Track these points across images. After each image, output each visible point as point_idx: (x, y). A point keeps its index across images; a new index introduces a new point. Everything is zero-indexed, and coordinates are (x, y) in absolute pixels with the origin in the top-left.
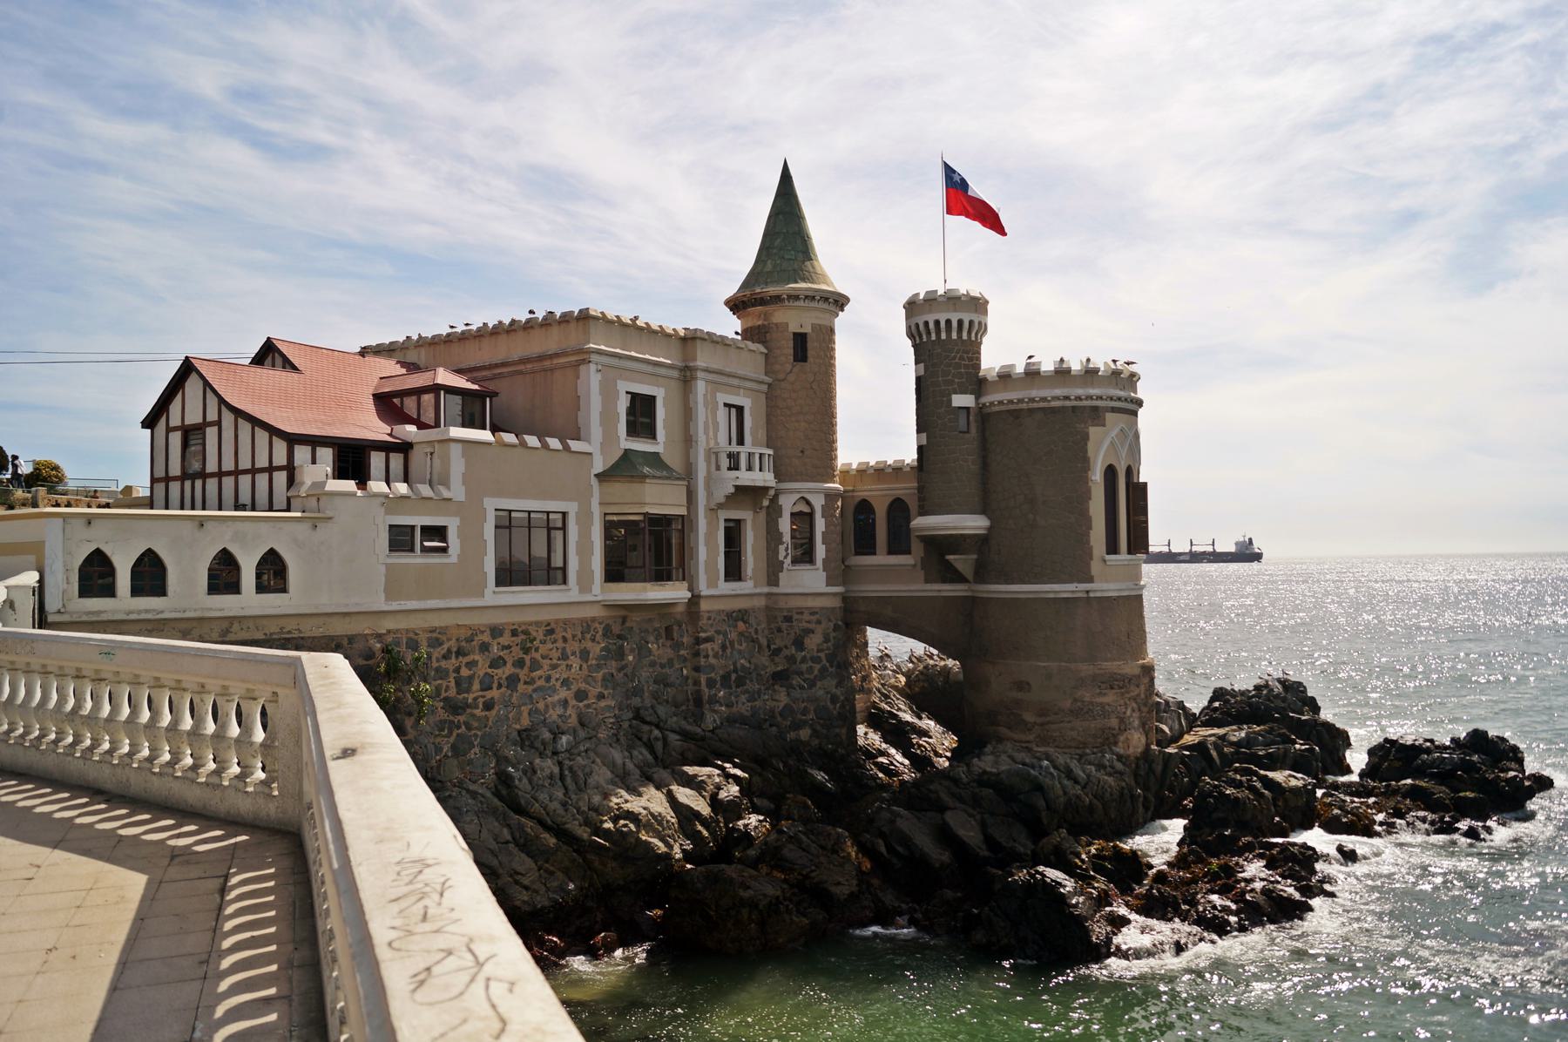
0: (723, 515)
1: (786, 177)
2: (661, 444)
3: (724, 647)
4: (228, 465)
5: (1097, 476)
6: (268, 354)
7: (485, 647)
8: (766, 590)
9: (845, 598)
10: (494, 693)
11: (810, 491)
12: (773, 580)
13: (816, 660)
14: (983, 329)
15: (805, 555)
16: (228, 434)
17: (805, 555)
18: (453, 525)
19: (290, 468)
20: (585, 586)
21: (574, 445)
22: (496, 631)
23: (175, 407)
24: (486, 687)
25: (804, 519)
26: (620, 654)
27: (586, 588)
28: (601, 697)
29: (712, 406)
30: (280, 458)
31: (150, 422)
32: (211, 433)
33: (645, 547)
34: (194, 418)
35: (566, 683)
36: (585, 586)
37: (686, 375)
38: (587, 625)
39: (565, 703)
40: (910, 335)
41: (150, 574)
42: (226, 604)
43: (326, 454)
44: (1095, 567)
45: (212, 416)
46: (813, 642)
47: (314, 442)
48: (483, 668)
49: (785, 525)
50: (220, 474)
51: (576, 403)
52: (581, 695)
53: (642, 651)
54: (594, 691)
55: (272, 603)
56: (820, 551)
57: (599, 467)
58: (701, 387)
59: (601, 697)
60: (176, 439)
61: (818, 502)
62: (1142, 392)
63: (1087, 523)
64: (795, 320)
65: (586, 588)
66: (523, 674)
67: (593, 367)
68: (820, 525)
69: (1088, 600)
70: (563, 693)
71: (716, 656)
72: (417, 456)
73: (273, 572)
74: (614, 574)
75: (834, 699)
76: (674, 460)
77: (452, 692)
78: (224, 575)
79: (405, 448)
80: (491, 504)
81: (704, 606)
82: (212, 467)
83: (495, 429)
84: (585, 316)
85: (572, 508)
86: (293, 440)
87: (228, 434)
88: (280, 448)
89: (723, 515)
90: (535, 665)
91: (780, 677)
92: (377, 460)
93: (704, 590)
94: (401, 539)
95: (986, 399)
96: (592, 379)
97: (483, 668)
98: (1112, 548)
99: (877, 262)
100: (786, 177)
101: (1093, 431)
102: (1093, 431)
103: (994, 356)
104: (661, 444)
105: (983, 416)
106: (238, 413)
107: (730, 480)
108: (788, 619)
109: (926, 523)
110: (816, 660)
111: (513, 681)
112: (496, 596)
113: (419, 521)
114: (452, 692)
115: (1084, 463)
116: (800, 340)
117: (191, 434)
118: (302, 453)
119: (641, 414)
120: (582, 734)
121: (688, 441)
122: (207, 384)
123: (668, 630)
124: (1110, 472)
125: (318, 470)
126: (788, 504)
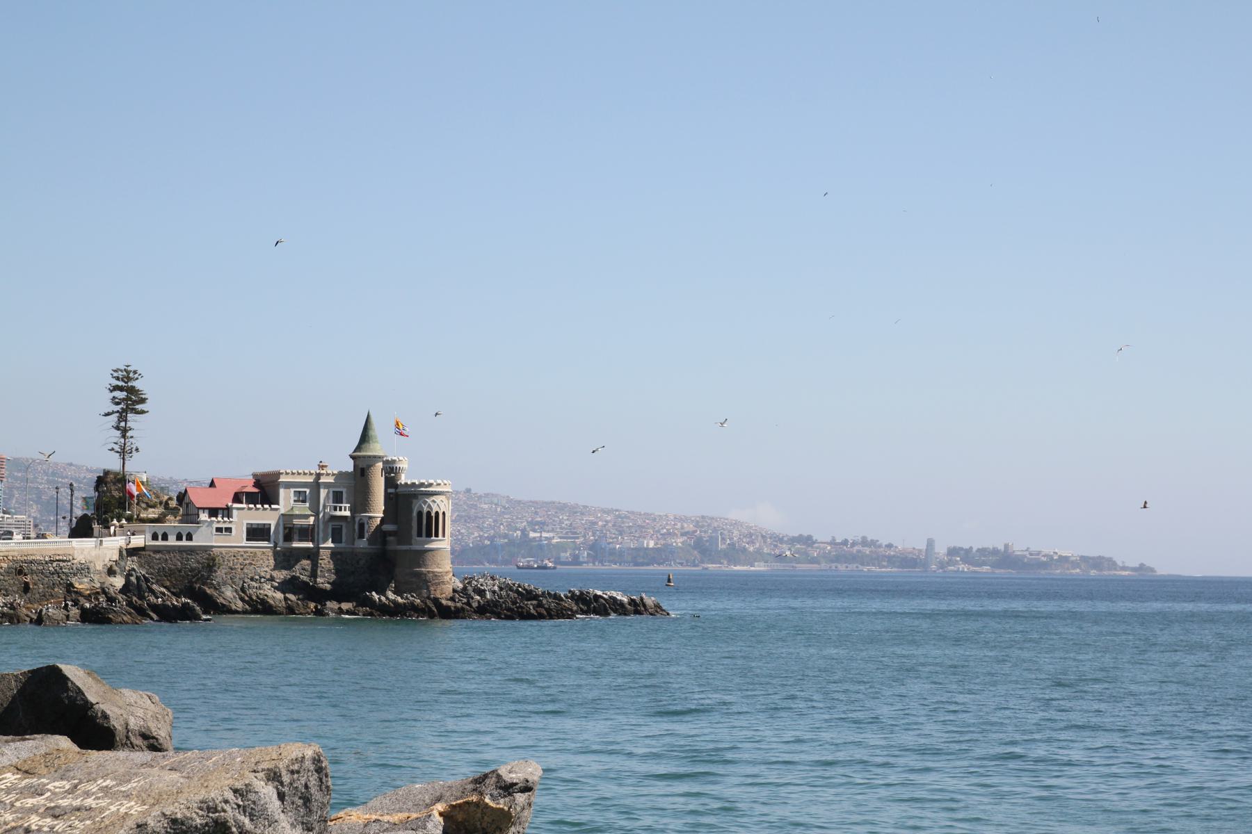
5: (415, 514)
6: (212, 484)
18: (233, 526)
46: (362, 562)
47: (204, 509)
49: (356, 527)
57: (282, 511)
63: (411, 527)
69: (411, 551)
80: (245, 522)
83: (248, 503)
89: (330, 524)
94: (219, 530)
98: (420, 535)
105: (397, 495)
112: (245, 543)
113: (224, 526)
115: (411, 511)
118: (201, 512)
125: (204, 516)
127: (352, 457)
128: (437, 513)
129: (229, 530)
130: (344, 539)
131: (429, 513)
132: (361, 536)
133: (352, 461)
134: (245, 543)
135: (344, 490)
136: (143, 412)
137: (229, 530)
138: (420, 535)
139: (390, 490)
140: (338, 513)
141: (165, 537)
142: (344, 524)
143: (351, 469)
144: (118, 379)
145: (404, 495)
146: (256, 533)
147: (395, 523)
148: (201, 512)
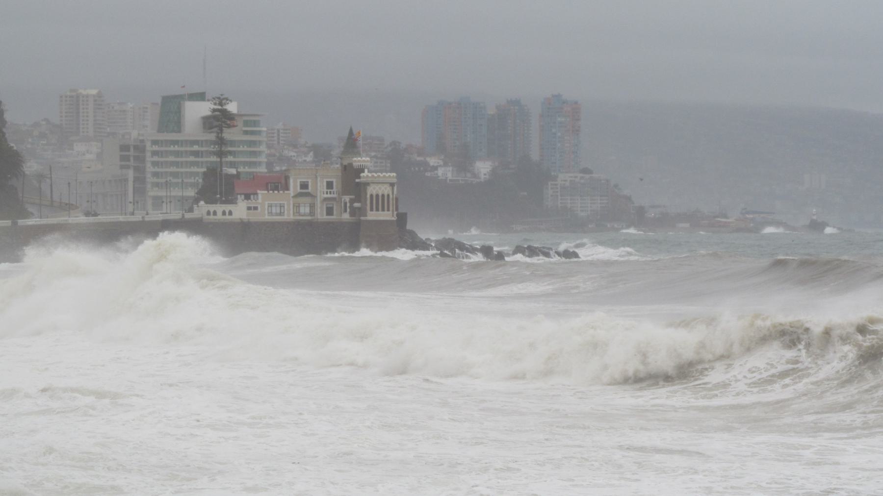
5: (368, 196)
17: (346, 211)
38: (289, 223)
41: (215, 213)
42: (224, 217)
43: (243, 196)
55: (230, 217)
56: (348, 210)
57: (292, 195)
73: (230, 213)
78: (224, 213)
89: (325, 203)
92: (252, 197)
98: (372, 210)
104: (310, 190)
115: (366, 194)
124: (372, 196)
130: (335, 213)
131: (377, 196)
135: (334, 180)
136: (234, 126)
137: (256, 208)
138: (372, 210)
142: (335, 203)
144: (215, 104)
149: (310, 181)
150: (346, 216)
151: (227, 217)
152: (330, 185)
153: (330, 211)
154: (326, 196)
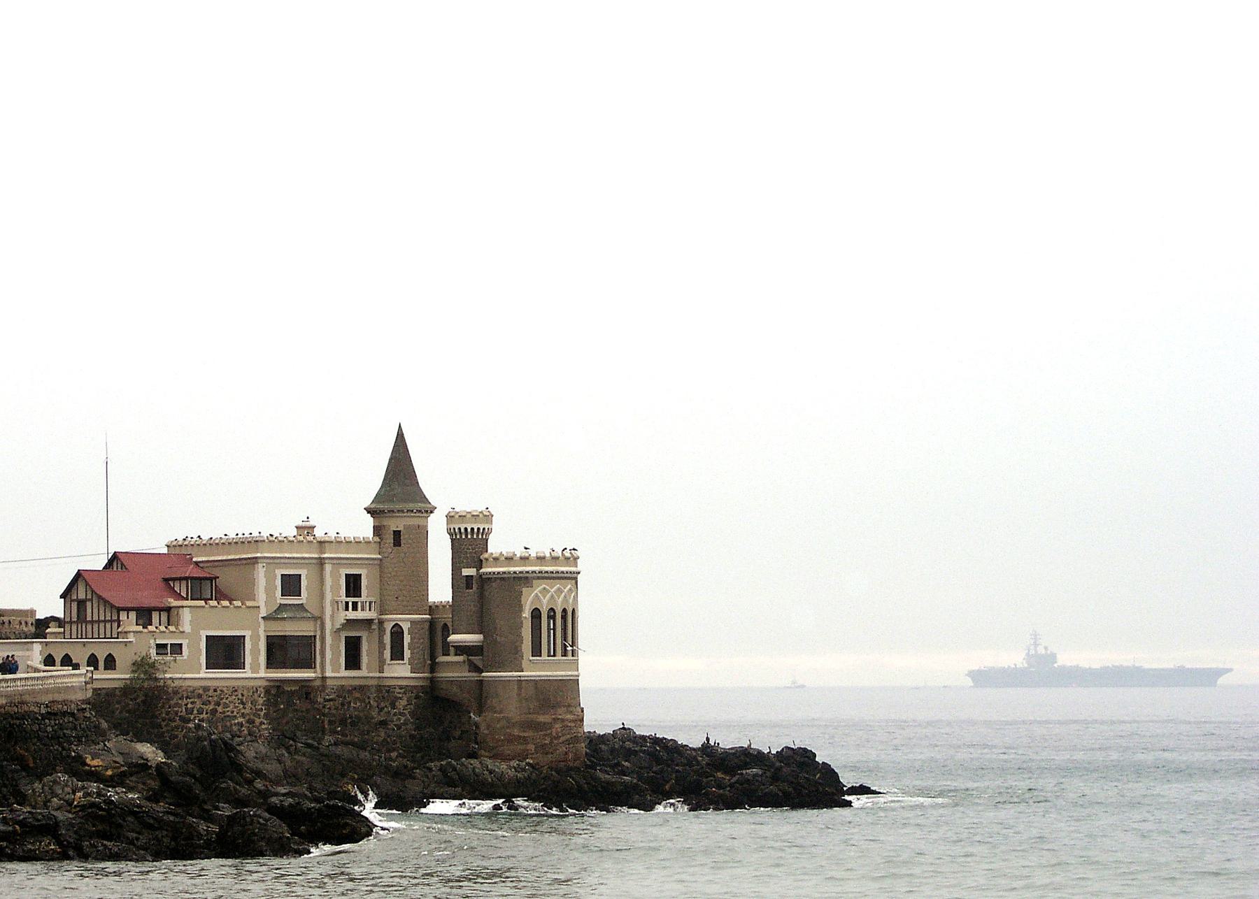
0: (343, 635)
1: (400, 437)
2: (303, 598)
3: (343, 704)
4: (96, 618)
5: (526, 614)
7: (200, 696)
8: (378, 675)
9: (432, 680)
10: (204, 716)
11: (401, 620)
12: (381, 671)
13: (401, 714)
14: (490, 531)
15: (397, 654)
16: (95, 605)
18: (185, 643)
19: (119, 621)
20: (255, 669)
21: (249, 603)
22: (206, 689)
23: (74, 591)
24: (200, 712)
25: (397, 633)
26: (276, 704)
27: (256, 669)
28: (262, 723)
29: (335, 576)
30: (115, 618)
31: (63, 596)
32: (89, 604)
33: (281, 651)
34: (82, 596)
35: (243, 715)
36: (255, 669)
37: (321, 562)
39: (241, 725)
40: (451, 534)
43: (133, 615)
44: (525, 664)
45: (89, 597)
48: (198, 705)
49: (387, 639)
50: (92, 622)
51: (252, 583)
52: (251, 722)
53: (289, 704)
54: (257, 721)
56: (407, 653)
57: (263, 613)
58: (328, 568)
59: (262, 723)
60: (74, 605)
61: (406, 627)
62: (581, 566)
64: (394, 524)
65: (256, 669)
66: (220, 709)
67: (260, 565)
68: (407, 639)
70: (241, 720)
71: (336, 709)
72: (174, 612)
74: (271, 664)
75: (412, 737)
76: (313, 609)
77: (184, 713)
79: (168, 610)
80: (204, 634)
81: (329, 682)
82: (89, 618)
84: (256, 543)
85: (247, 634)
86: (119, 610)
87: (95, 605)
88: (115, 612)
90: (226, 706)
91: (383, 723)
92: (155, 616)
93: (328, 674)
95: (483, 570)
96: (260, 572)
97: (198, 705)
98: (537, 651)
99: (445, 488)
100: (400, 437)
101: (524, 590)
102: (524, 590)
103: (496, 546)
104: (303, 598)
106: (100, 597)
107: (344, 616)
108: (388, 692)
109: (453, 638)
110: (401, 714)
111: (214, 711)
112: (204, 673)
114: (184, 713)
116: (397, 534)
117: (81, 604)
118: (123, 616)
119: (291, 585)
120: (249, 738)
121: (322, 596)
122: (87, 584)
123: (308, 694)
124: (536, 614)
126: (388, 627)
127: (369, 510)
128: (564, 611)
129: (177, 649)
132: (397, 654)
133: (369, 521)
134: (204, 673)
137: (177, 649)
139: (466, 572)
140: (359, 615)
141: (93, 661)
142: (364, 635)
143: (369, 534)
145: (503, 579)
146: (225, 652)
147: (480, 626)
148: (123, 616)
149: (304, 573)
150: (400, 671)
151: (101, 675)
152: (353, 585)
153: (353, 660)
154: (352, 615)
